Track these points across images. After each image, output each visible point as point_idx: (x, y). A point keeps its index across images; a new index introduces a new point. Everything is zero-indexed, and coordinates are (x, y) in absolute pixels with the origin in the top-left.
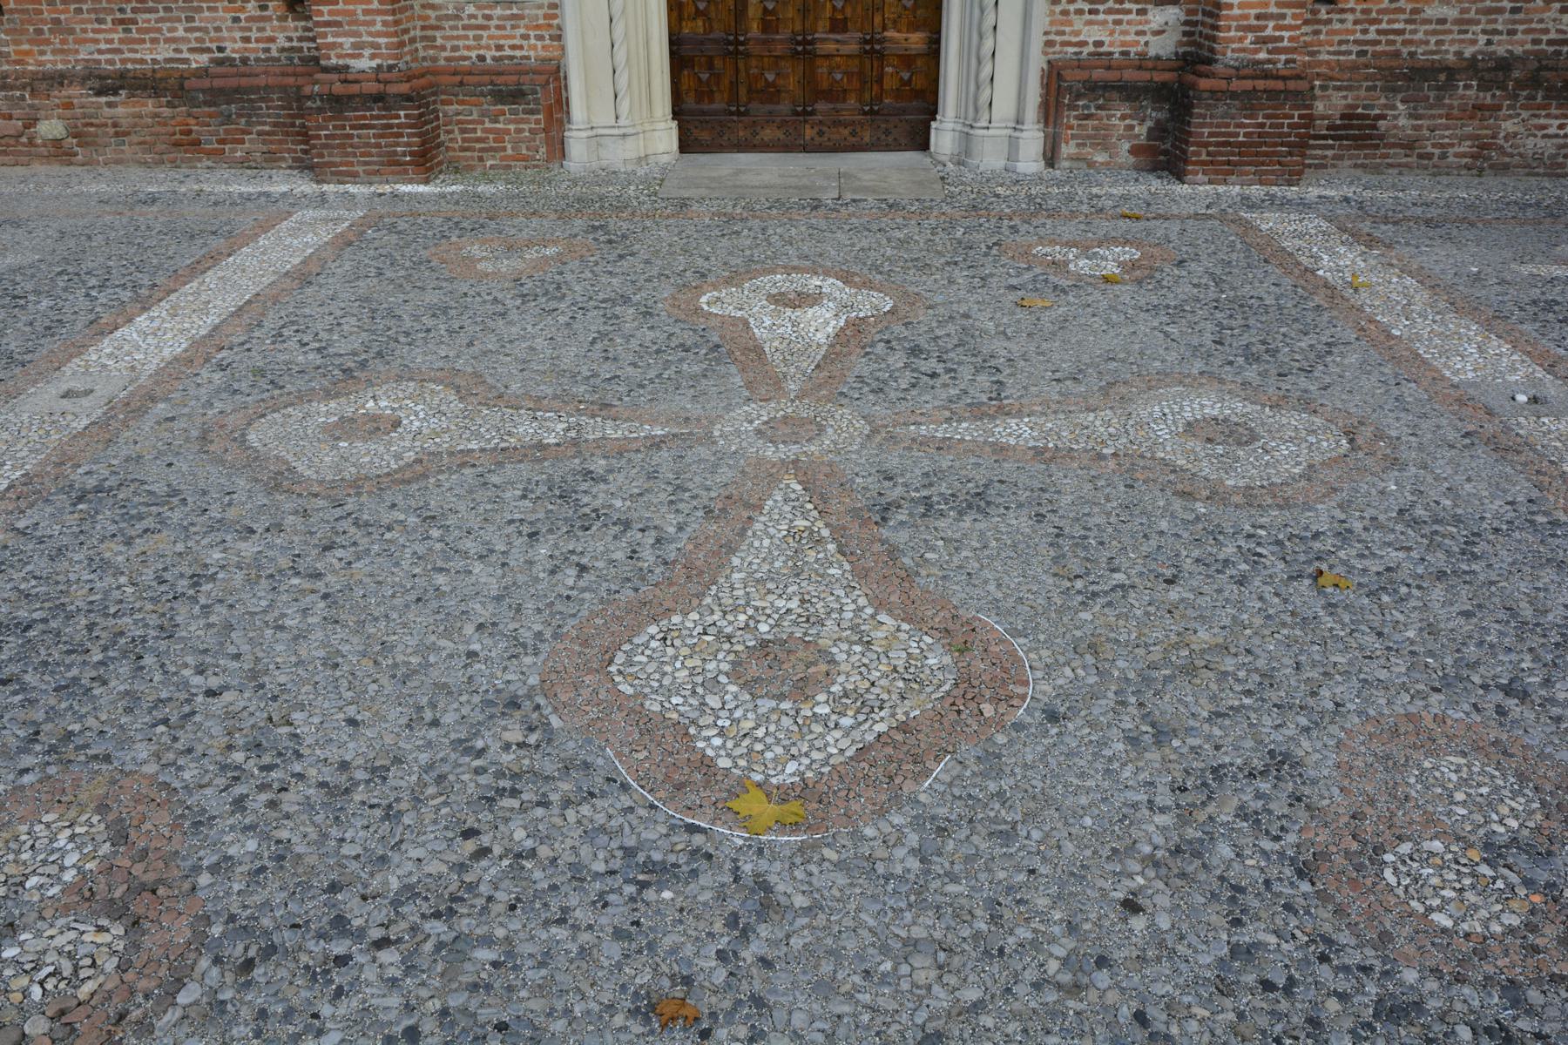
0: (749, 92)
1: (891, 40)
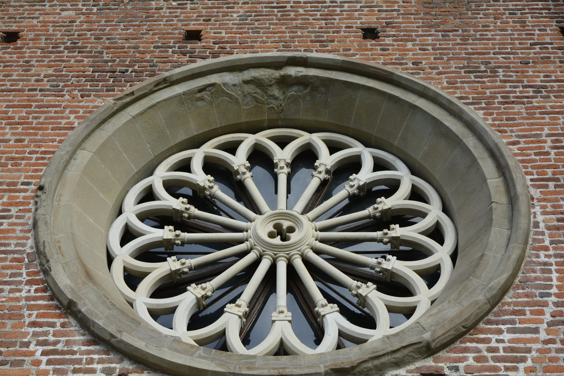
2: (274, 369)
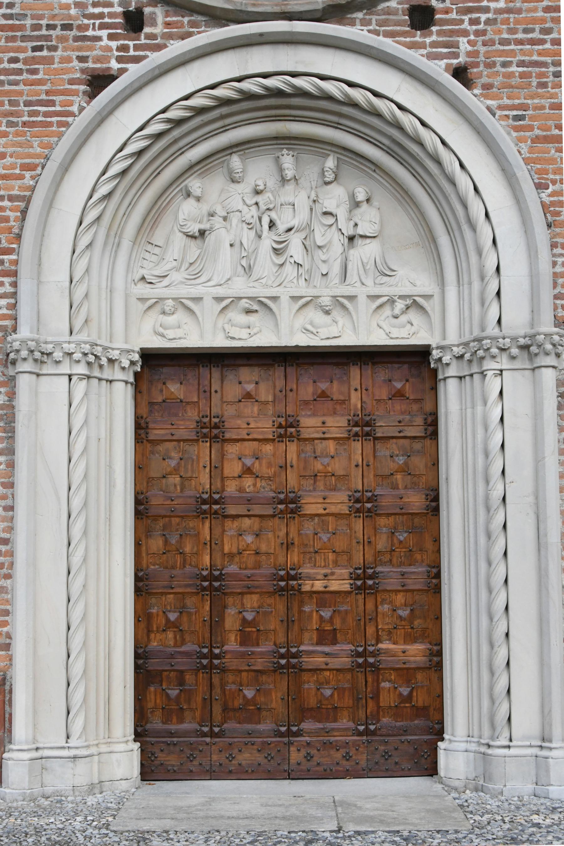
0: (225, 709)
1: (387, 652)
2: (276, 5)
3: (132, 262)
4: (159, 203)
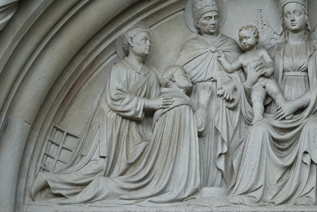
3: (28, 159)
4: (77, 64)
